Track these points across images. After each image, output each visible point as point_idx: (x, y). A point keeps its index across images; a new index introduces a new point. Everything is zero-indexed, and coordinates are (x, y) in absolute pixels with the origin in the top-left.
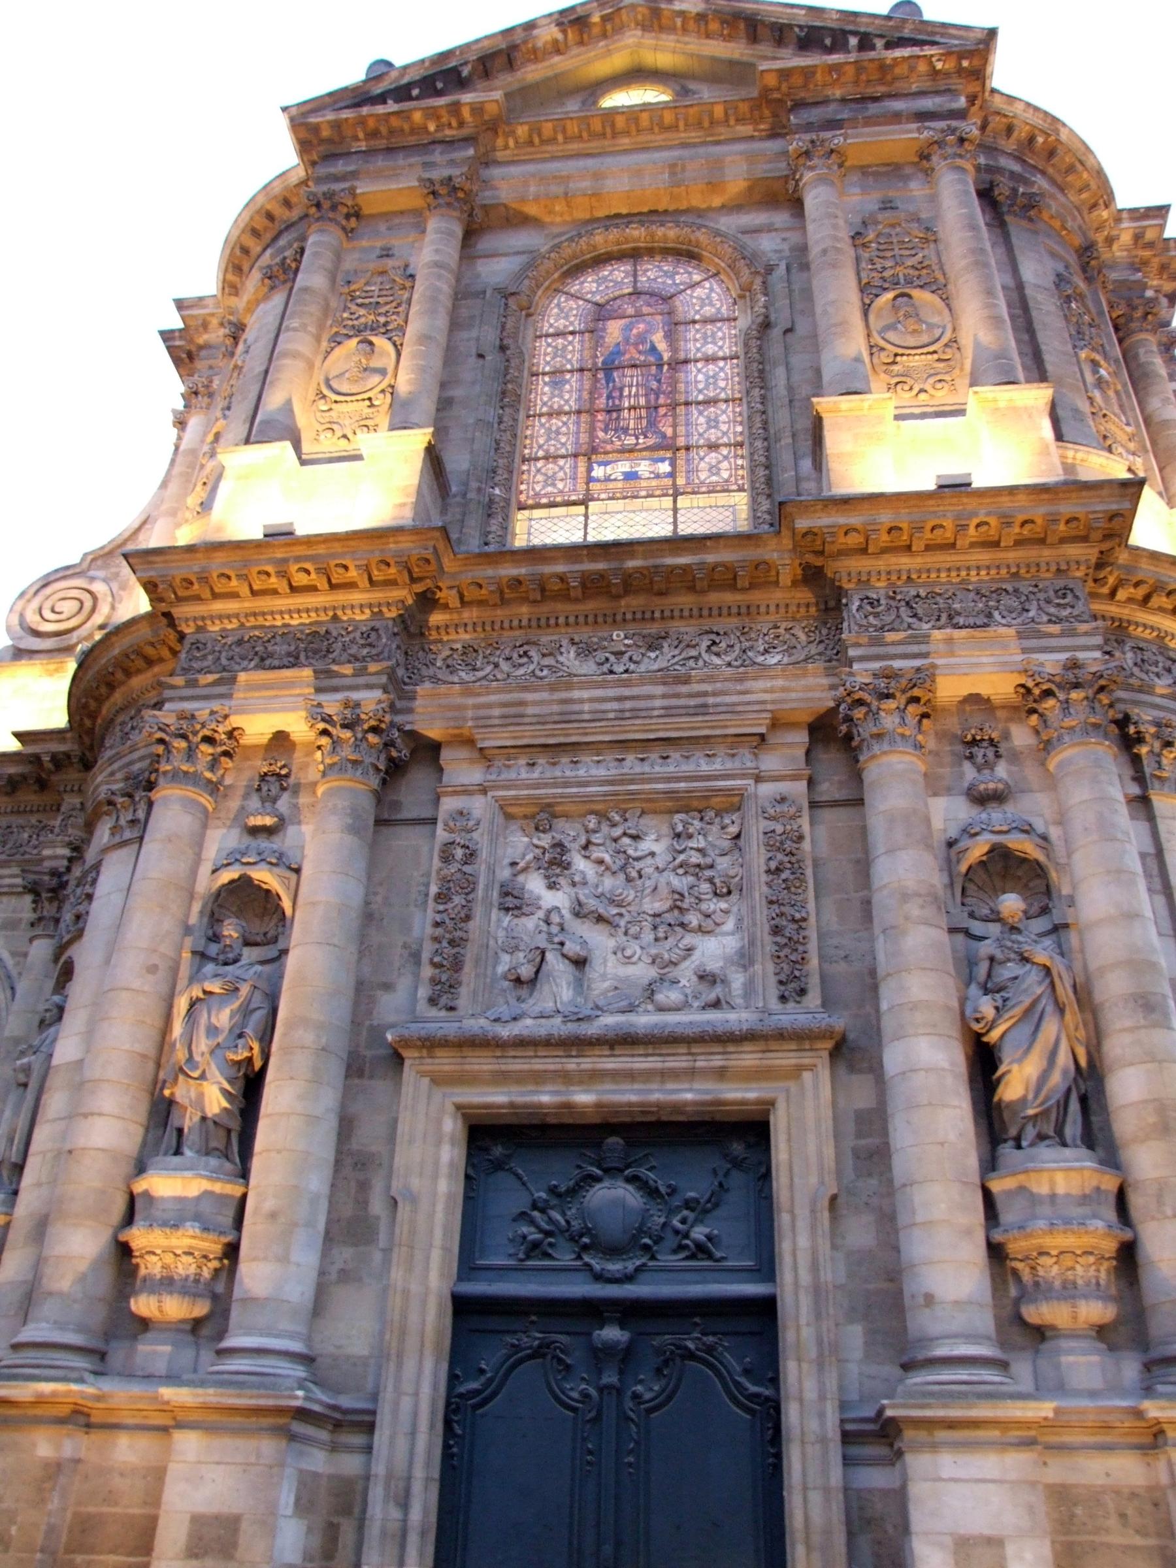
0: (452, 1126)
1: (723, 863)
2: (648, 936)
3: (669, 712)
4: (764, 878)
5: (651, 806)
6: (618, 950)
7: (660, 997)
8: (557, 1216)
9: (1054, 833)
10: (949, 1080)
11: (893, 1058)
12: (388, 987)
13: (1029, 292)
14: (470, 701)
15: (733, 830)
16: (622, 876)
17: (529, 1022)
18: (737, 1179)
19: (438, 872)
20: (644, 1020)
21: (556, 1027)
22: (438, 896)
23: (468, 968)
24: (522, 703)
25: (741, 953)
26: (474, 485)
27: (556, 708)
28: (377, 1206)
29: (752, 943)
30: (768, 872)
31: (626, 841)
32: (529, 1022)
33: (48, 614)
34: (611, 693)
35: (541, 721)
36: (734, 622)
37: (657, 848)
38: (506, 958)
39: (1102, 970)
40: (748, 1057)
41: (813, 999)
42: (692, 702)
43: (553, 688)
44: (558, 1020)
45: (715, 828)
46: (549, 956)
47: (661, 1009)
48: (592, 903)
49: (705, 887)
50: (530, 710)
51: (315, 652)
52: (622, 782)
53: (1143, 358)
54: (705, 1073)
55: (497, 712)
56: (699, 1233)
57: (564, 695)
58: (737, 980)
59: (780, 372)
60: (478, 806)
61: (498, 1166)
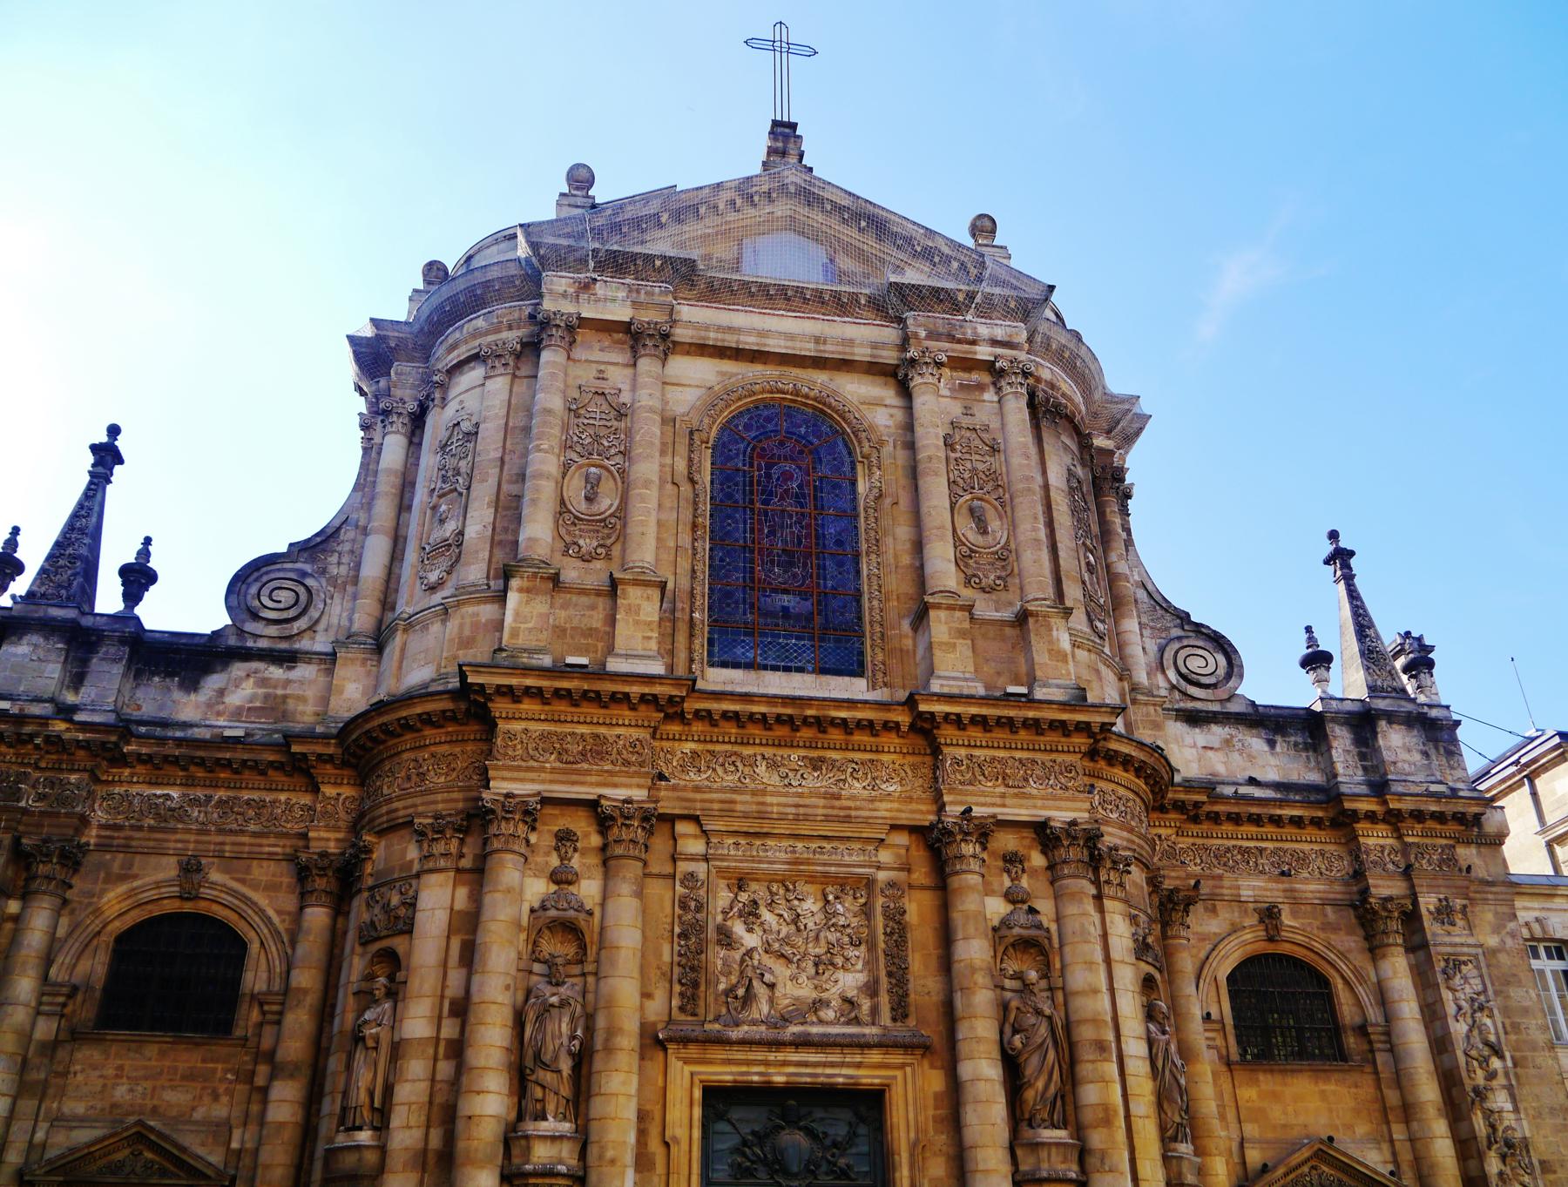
0: (698, 1094)
3: (827, 819)
4: (882, 937)
5: (811, 879)
6: (793, 978)
7: (822, 1014)
9: (1053, 927)
11: (966, 1070)
13: (1053, 494)
14: (698, 796)
15: (862, 901)
16: (793, 927)
17: (746, 1028)
18: (862, 1130)
19: (680, 917)
20: (815, 1030)
21: (762, 1031)
23: (703, 988)
24: (732, 802)
25: (866, 985)
27: (754, 807)
28: (655, 1146)
30: (885, 933)
31: (796, 902)
34: (791, 800)
35: (746, 816)
37: (815, 908)
38: (723, 979)
39: (1079, 1022)
40: (875, 1056)
41: (912, 1022)
42: (842, 813)
43: (754, 793)
46: (755, 983)
47: (821, 1022)
49: (846, 939)
50: (739, 807)
53: (1109, 517)
54: (849, 1065)
55: (716, 806)
56: (842, 1162)
57: (761, 799)
58: (866, 1004)
59: (889, 540)
60: (700, 869)
61: (721, 1117)
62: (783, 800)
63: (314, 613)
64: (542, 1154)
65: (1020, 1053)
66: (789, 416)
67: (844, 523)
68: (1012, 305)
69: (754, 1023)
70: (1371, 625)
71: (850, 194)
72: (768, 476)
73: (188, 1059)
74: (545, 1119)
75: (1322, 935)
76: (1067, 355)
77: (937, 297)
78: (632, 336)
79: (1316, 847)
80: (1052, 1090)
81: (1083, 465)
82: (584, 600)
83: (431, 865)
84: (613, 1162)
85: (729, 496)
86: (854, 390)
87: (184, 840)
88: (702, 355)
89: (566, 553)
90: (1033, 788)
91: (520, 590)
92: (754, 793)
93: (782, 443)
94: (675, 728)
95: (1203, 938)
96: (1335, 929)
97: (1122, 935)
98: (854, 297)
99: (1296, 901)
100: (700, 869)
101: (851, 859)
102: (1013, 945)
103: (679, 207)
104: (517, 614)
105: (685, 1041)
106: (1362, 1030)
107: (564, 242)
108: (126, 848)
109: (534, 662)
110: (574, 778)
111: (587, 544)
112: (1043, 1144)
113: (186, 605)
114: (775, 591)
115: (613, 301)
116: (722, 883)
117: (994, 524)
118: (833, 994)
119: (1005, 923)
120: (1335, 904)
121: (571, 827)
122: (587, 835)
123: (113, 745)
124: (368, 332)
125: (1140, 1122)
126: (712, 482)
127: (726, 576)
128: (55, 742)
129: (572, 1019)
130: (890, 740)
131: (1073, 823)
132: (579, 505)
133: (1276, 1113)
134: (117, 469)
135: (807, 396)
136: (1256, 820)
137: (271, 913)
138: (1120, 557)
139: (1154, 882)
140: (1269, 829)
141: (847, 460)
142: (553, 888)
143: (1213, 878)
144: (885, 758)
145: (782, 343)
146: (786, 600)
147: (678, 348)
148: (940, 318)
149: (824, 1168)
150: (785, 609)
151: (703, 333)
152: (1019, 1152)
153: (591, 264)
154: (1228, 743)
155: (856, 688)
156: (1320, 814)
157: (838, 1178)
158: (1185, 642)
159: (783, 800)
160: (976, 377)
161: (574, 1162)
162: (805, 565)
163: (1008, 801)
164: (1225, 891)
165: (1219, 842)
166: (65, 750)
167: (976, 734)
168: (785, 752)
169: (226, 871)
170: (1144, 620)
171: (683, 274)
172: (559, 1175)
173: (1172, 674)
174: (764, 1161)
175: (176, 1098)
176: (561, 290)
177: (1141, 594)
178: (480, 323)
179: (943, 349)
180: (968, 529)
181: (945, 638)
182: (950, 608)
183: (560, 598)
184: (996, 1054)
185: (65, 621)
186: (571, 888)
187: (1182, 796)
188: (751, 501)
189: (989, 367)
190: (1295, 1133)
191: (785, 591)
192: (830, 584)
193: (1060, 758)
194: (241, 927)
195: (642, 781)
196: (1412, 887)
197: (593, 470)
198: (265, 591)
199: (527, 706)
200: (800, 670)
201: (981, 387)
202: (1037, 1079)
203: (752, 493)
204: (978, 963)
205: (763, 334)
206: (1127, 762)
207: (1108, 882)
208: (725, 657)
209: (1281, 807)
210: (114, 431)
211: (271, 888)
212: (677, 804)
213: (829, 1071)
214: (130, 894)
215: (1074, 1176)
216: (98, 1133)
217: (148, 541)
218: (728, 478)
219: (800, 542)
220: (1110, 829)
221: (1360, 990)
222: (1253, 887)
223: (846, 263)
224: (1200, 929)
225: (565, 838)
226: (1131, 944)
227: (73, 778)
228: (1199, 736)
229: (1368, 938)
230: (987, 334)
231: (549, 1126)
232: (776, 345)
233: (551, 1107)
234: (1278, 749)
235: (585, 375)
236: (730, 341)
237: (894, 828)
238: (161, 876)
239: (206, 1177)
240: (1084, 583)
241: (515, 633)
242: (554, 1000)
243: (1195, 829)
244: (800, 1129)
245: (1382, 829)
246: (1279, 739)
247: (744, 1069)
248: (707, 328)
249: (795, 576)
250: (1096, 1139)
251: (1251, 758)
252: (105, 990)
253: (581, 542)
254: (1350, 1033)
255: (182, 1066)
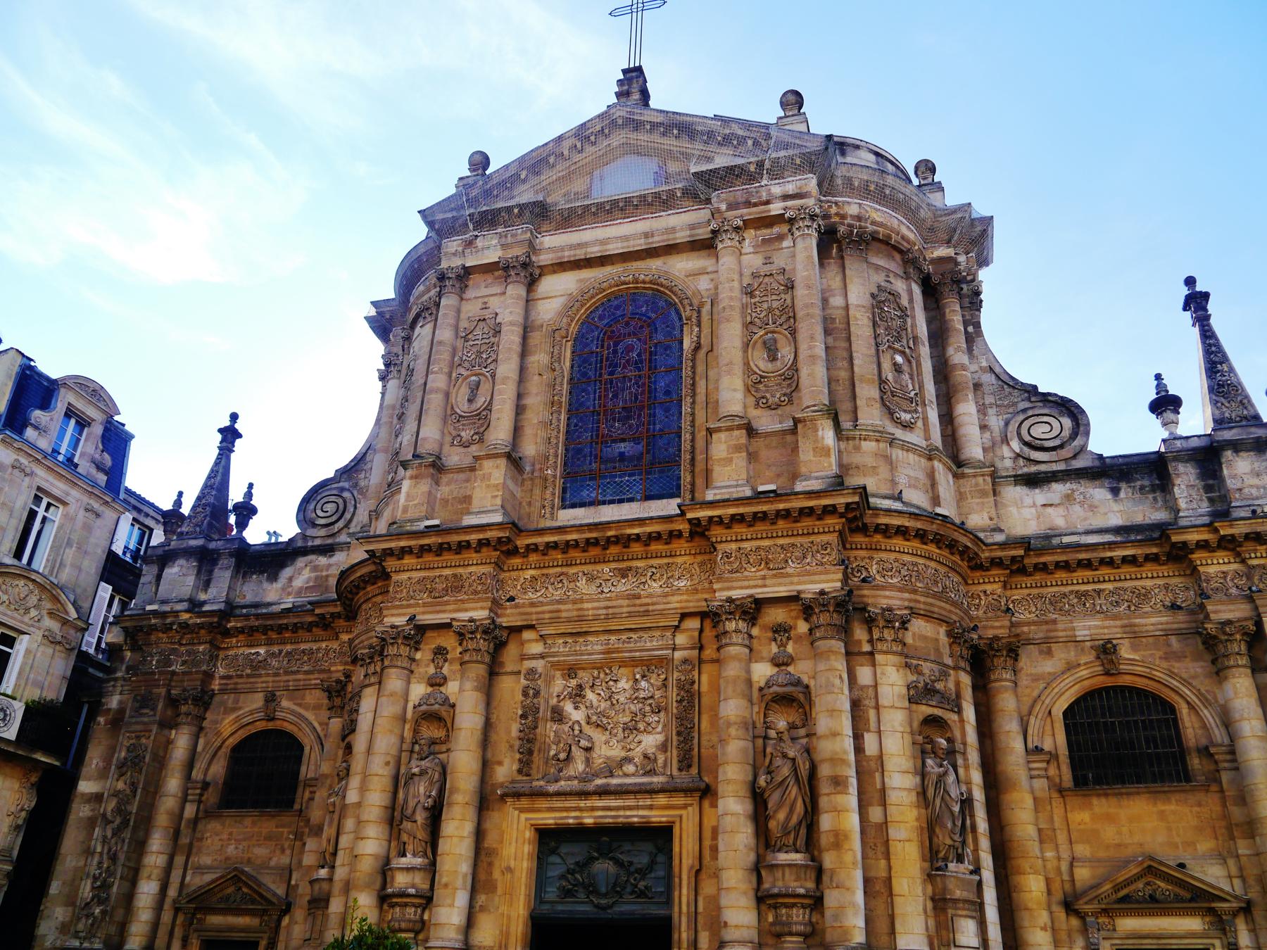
0: (529, 834)
1: (658, 694)
2: (621, 735)
5: (623, 664)
6: (607, 742)
8: (578, 876)
10: (742, 818)
12: (500, 763)
13: (851, 312)
14: (534, 610)
15: (663, 677)
20: (614, 781)
22: (521, 716)
23: (535, 754)
26: (538, 467)
27: (575, 613)
29: (666, 740)
32: (563, 783)
33: (320, 513)
35: (569, 620)
36: (666, 561)
37: (627, 686)
38: (554, 747)
39: (823, 761)
40: (662, 800)
41: (694, 771)
42: (642, 609)
43: (574, 602)
44: (576, 782)
45: (655, 676)
47: (626, 775)
48: (594, 718)
49: (648, 708)
50: (564, 615)
51: (456, 587)
52: (608, 653)
53: (948, 316)
54: (643, 808)
55: (547, 616)
56: (642, 884)
57: (579, 606)
60: (539, 665)
61: (553, 852)
62: (596, 604)
63: (348, 516)
64: (401, 881)
65: (764, 790)
66: (634, 300)
67: (672, 376)
68: (798, 161)
69: (569, 779)
70: (1225, 359)
71: (661, 111)
72: (615, 352)
73: (268, 826)
74: (404, 855)
75: (1165, 665)
76: (872, 187)
77: (732, 174)
78: (500, 270)
79: (1160, 582)
80: (795, 820)
81: (907, 277)
82: (462, 476)
83: (367, 682)
84: (446, 885)
85: (584, 375)
86: (680, 266)
87: (266, 681)
88: (565, 270)
89: (452, 445)
90: (792, 568)
91: (411, 478)
92: (574, 602)
93: (627, 324)
94: (517, 561)
95: (1036, 678)
96: (1179, 657)
97: (891, 680)
98: (671, 193)
99: (1135, 636)
100: (539, 665)
101: (652, 644)
102: (773, 700)
103: (536, 162)
104: (408, 495)
105: (518, 795)
106: (1205, 752)
107: (449, 215)
108: (235, 691)
109: (414, 528)
110: (438, 608)
111: (466, 435)
112: (777, 866)
113: (275, 521)
114: (614, 441)
115: (490, 249)
116: (558, 674)
117: (785, 352)
118: (637, 753)
119: (769, 684)
120: (1178, 633)
121: (444, 644)
122: (454, 649)
123: (221, 625)
124: (373, 312)
125: (900, 845)
126: (572, 367)
127: (579, 437)
128: (185, 626)
129: (431, 783)
130: (681, 545)
131: (822, 593)
132: (462, 406)
133: (1109, 833)
134: (238, 441)
135: (644, 282)
136: (1088, 565)
137: (316, 725)
138: (958, 349)
139: (955, 637)
140: (1105, 571)
141: (678, 324)
142: (430, 689)
143: (1047, 623)
144: (679, 560)
145: (620, 245)
146: (623, 447)
147: (545, 270)
148: (738, 191)
149: (629, 889)
150: (622, 454)
151: (560, 254)
152: (763, 873)
153: (471, 227)
154: (1069, 498)
155: (669, 506)
156: (1155, 550)
157: (638, 897)
158: (1030, 413)
159: (596, 604)
160: (776, 230)
161: (426, 886)
162: (639, 415)
163: (768, 582)
164: (1061, 634)
165: (1056, 589)
166: (192, 632)
167: (740, 530)
168: (599, 567)
169: (290, 699)
170: (989, 400)
171: (540, 213)
172: (409, 896)
173: (1016, 445)
174: (585, 886)
175: (260, 852)
176: (453, 250)
177: (988, 379)
178: (422, 288)
179: (736, 217)
180: (760, 361)
181: (724, 454)
182: (730, 429)
183: (445, 478)
184: (744, 791)
185: (198, 547)
186: (442, 689)
187: (999, 554)
188: (601, 375)
189: (780, 219)
190: (1129, 852)
191: (623, 440)
192: (658, 427)
193: (818, 539)
194: (299, 735)
195: (485, 604)
196: (1256, 608)
197: (473, 378)
198: (319, 506)
199: (408, 561)
200: (631, 500)
201: (781, 238)
202: (775, 812)
203: (601, 368)
204: (733, 719)
205: (603, 242)
206: (902, 532)
207: (880, 639)
208: (576, 500)
209: (1110, 549)
210: (234, 417)
211: (317, 707)
212: (519, 618)
213: (628, 813)
214: (237, 719)
215: (802, 891)
216: (214, 876)
217: (251, 486)
218: (585, 361)
219: (636, 398)
220: (887, 593)
221: (1206, 713)
222: (1088, 627)
223: (673, 167)
224: (1034, 671)
225: (440, 652)
226: (904, 690)
227: (201, 648)
228: (1039, 496)
229: (1214, 662)
230: (776, 193)
231: (408, 860)
232: (615, 248)
233: (410, 848)
234: (1122, 495)
235: (471, 309)
236: (580, 254)
237: (684, 616)
238: (255, 706)
239: (273, 904)
240: (882, 382)
241: (405, 510)
242: (416, 770)
243: (1029, 581)
244: (610, 859)
245: (1222, 556)
246: (1123, 485)
247: (565, 814)
248: (562, 249)
249: (630, 426)
250: (828, 860)
251: (1093, 508)
252: (224, 783)
253: (463, 434)
254: (1194, 755)
255: (264, 831)
